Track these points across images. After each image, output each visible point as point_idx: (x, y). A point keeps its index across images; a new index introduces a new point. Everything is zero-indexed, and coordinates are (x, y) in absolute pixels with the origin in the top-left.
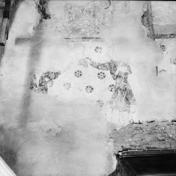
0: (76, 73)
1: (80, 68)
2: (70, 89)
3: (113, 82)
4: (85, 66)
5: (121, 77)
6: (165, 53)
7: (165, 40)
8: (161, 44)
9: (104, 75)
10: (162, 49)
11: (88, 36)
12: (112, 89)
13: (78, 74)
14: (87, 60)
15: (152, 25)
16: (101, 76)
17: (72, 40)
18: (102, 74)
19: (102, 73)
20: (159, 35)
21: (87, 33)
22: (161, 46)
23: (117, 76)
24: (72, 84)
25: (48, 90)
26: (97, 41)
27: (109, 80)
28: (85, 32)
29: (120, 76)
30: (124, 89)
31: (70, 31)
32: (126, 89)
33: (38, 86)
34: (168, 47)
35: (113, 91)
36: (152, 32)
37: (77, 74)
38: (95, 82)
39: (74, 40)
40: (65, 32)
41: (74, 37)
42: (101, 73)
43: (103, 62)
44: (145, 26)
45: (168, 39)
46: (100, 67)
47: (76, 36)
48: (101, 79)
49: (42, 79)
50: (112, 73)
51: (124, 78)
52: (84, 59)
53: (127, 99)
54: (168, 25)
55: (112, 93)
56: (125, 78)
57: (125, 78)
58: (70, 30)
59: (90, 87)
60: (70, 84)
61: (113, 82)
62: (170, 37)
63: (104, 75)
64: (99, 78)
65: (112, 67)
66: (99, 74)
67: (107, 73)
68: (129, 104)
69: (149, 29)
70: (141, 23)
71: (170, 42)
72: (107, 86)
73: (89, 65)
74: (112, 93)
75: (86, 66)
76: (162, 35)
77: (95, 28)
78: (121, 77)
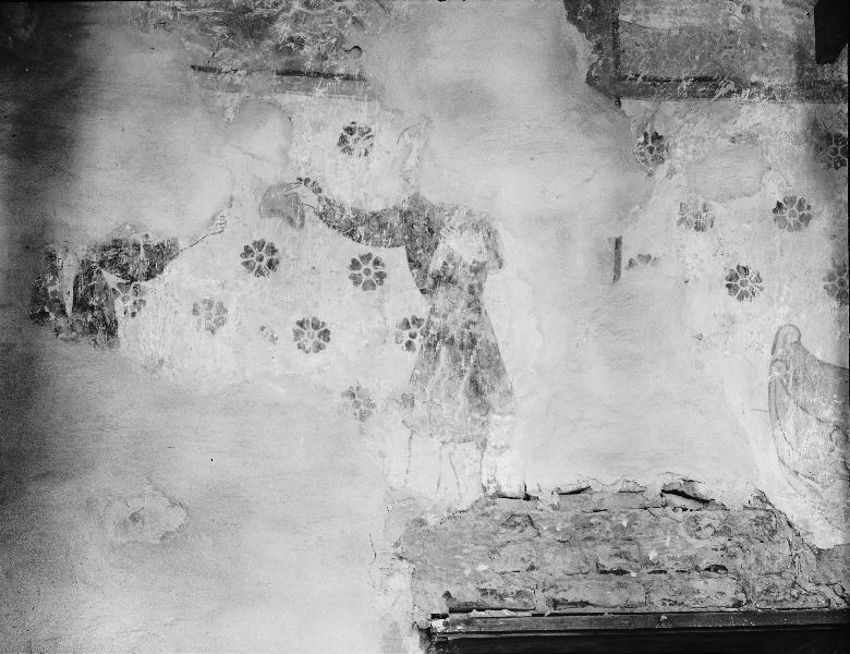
0: (248, 251)
1: (269, 230)
2: (223, 332)
3: (420, 306)
4: (291, 221)
5: (455, 283)
6: (661, 171)
7: (669, 106)
8: (648, 130)
9: (380, 269)
10: (651, 150)
11: (309, 65)
12: (413, 336)
13: (261, 259)
14: (301, 190)
15: (616, 24)
16: (367, 272)
17: (227, 78)
18: (370, 265)
19: (371, 262)
20: (644, 78)
21: (300, 43)
22: (646, 135)
23: (437, 279)
24: (231, 310)
25: (120, 332)
26: (349, 93)
27: (403, 295)
28: (291, 39)
29: (450, 278)
31: (217, 29)
32: (474, 342)
33: (69, 310)
34: (675, 145)
35: (418, 349)
36: (611, 60)
38: (341, 305)
39: (238, 80)
40: (193, 31)
41: (237, 62)
43: (377, 206)
44: (582, 28)
45: (682, 104)
46: (361, 230)
47: (246, 59)
48: (365, 288)
49: (89, 274)
50: (414, 263)
51: (466, 288)
52: (288, 186)
53: (476, 388)
54: (691, 29)
55: (412, 358)
56: (471, 290)
57: (471, 287)
58: (218, 23)
59: (316, 327)
60: (222, 309)
61: (420, 306)
62: (692, 93)
63: (380, 269)
64: (356, 283)
65: (416, 229)
66: (355, 264)
67: (395, 259)
68: (486, 408)
69: (599, 47)
70: (565, 13)
71: (689, 116)
72: (393, 321)
73: (309, 214)
74: (412, 358)
75: (298, 222)
76: (655, 80)
77: (339, 20)
78: (455, 283)
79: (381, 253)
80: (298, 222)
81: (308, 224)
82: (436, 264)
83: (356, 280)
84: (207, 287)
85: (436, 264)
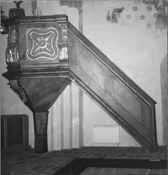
0: (133, 8)
4: (139, 3)
18: (150, 8)
23: (159, 8)
25: (118, 20)
30: (163, 16)
33: (111, 18)
37: (134, 9)
42: (149, 7)
46: (148, 3)
50: (156, 7)
55: (156, 19)
56: (163, 9)
59: (143, 16)
60: (130, 15)
61: (156, 12)
66: (148, 8)
67: (153, 6)
72: (153, 15)
79: (151, 6)
80: (140, 3)
81: (141, 3)
82: (159, 6)
83: (148, 10)
84: (129, 13)
85: (159, 6)
